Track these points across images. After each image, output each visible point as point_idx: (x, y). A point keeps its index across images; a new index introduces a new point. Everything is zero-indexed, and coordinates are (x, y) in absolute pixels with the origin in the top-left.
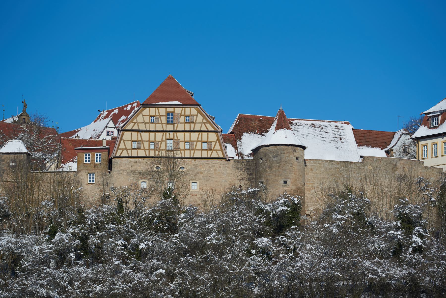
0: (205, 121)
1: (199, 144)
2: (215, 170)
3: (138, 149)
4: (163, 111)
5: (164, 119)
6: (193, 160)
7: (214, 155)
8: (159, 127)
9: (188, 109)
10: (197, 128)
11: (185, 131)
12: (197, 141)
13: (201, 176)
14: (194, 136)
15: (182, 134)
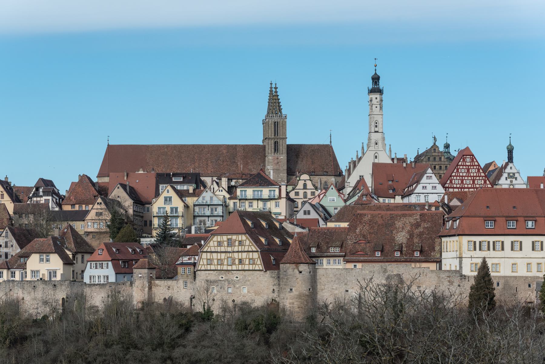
0: (251, 244)
1: (247, 260)
2: (257, 278)
3: (211, 264)
4: (225, 238)
5: (226, 244)
6: (243, 272)
7: (257, 268)
8: (223, 249)
9: (240, 236)
10: (246, 249)
11: (238, 252)
12: (246, 258)
13: (248, 283)
14: (244, 255)
15: (237, 254)
